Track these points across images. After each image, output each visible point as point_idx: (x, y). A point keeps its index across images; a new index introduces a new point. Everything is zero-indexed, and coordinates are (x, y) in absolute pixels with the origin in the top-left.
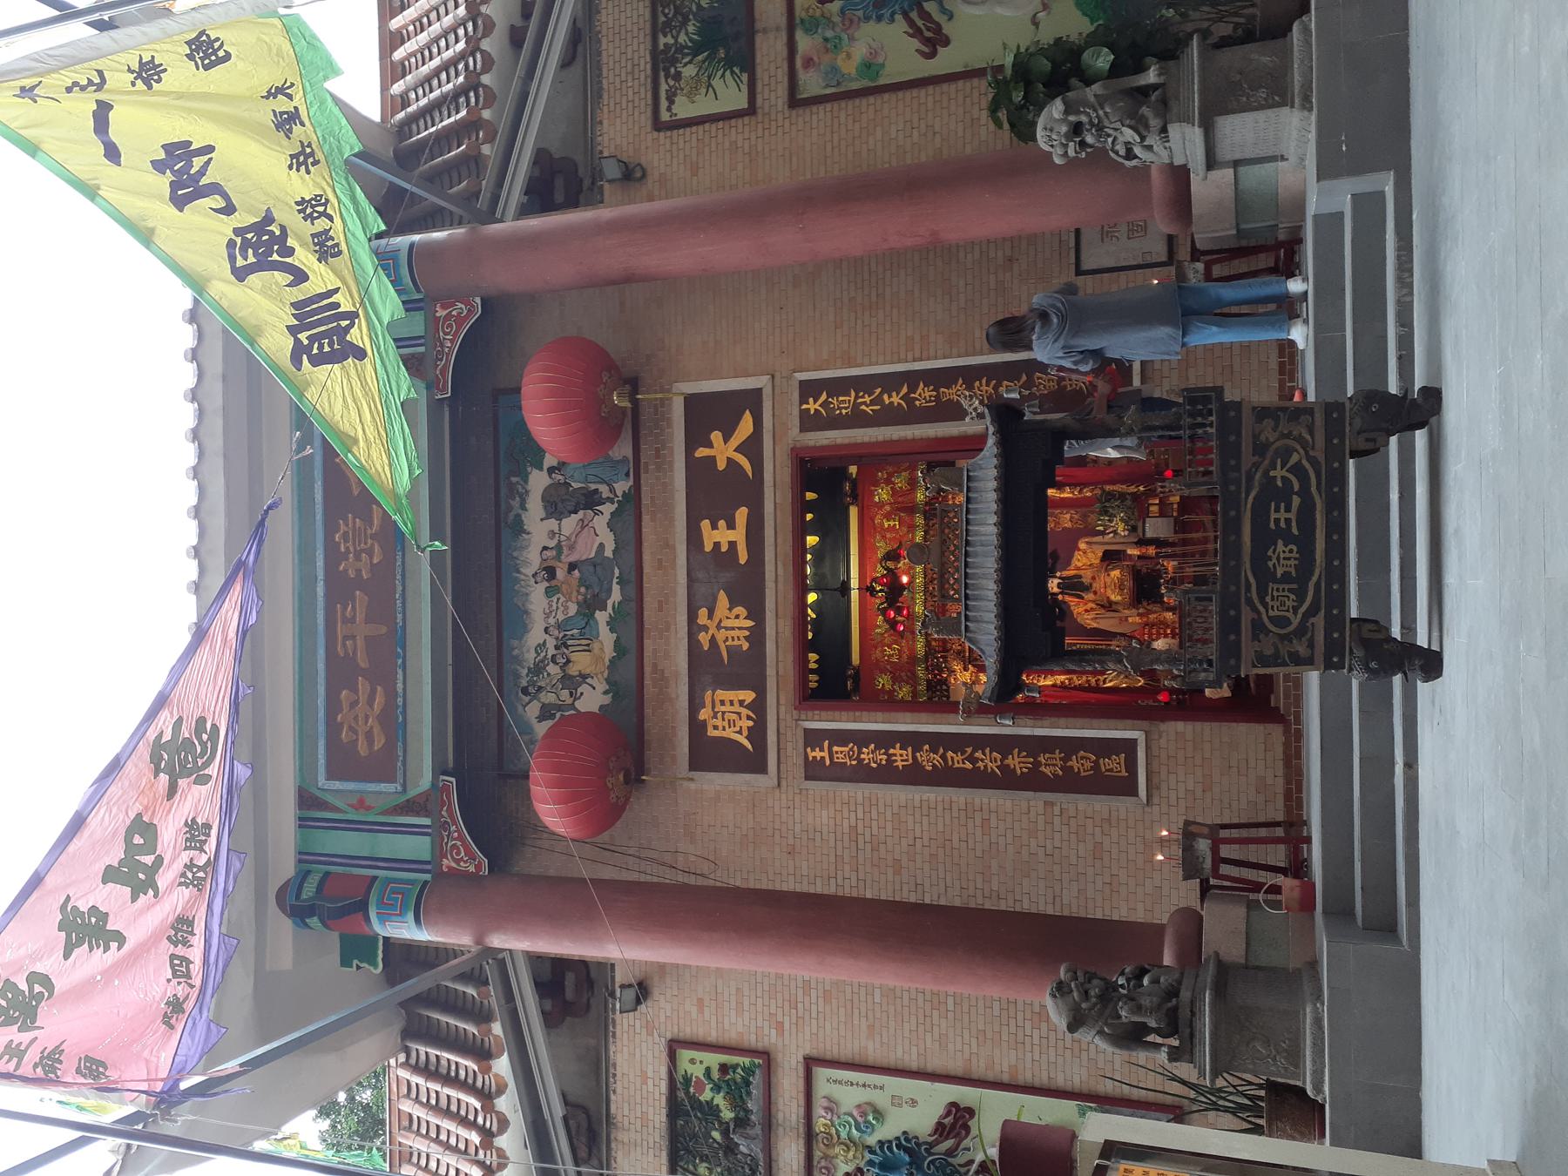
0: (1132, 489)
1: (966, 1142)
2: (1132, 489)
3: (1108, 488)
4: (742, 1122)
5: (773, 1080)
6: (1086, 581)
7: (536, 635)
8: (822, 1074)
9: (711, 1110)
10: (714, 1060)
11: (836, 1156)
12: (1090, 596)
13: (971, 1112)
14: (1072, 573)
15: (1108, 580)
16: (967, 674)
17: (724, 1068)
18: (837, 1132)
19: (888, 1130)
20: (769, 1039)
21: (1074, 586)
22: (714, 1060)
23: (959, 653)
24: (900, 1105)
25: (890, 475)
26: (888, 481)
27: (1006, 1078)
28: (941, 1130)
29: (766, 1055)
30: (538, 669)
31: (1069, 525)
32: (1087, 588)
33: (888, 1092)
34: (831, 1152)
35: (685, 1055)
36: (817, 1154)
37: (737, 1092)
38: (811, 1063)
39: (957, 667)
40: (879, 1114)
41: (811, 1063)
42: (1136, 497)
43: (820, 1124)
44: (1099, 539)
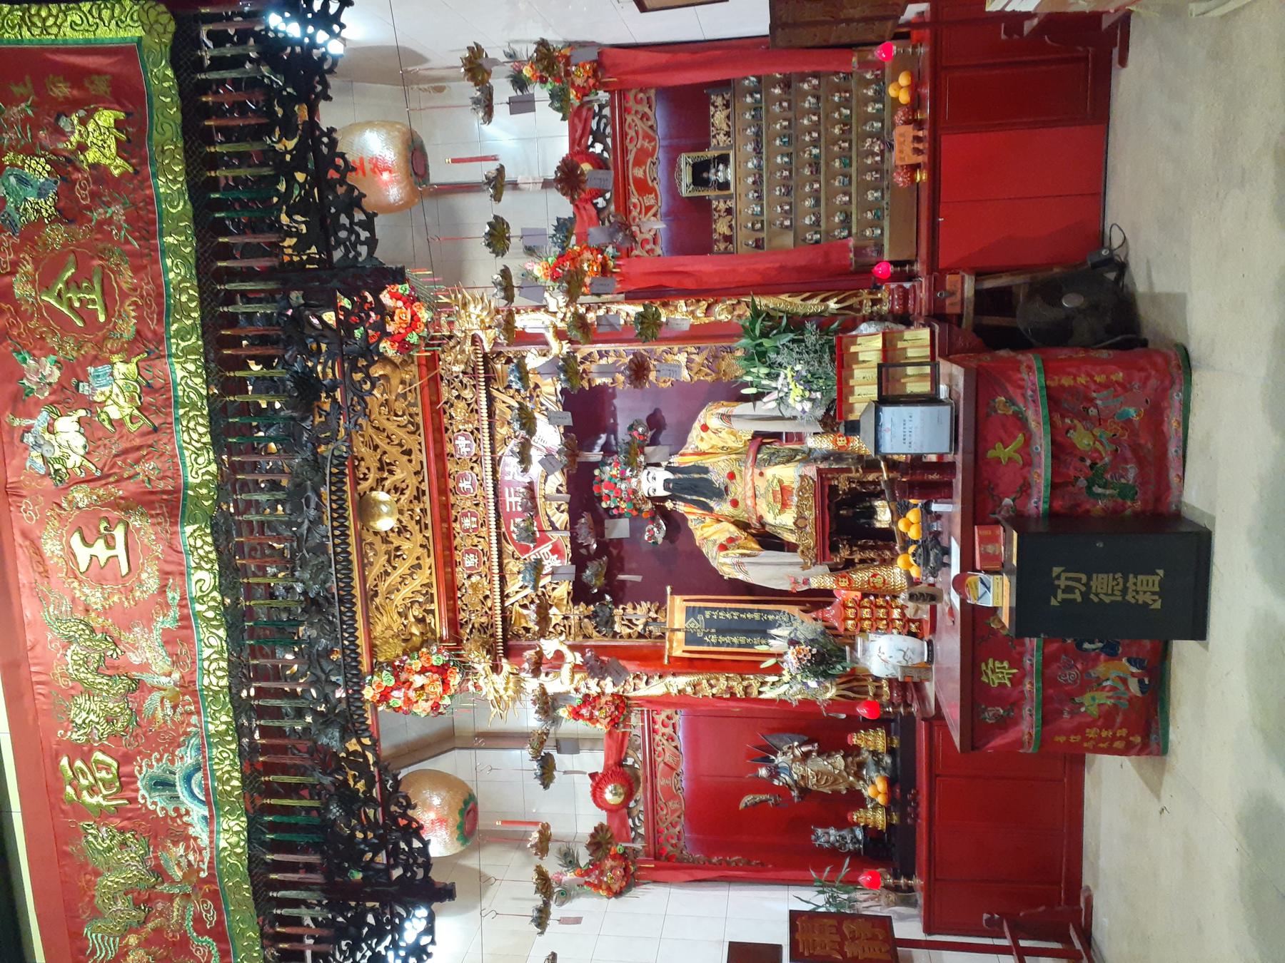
0: (814, 305)
2: (814, 305)
3: (763, 302)
6: (718, 476)
12: (724, 508)
14: (689, 461)
15: (761, 484)
16: (499, 680)
21: (695, 486)
23: (484, 628)
25: (73, 372)
26: (67, 396)
31: (685, 375)
32: (720, 494)
39: (481, 663)
42: (823, 322)
44: (744, 408)
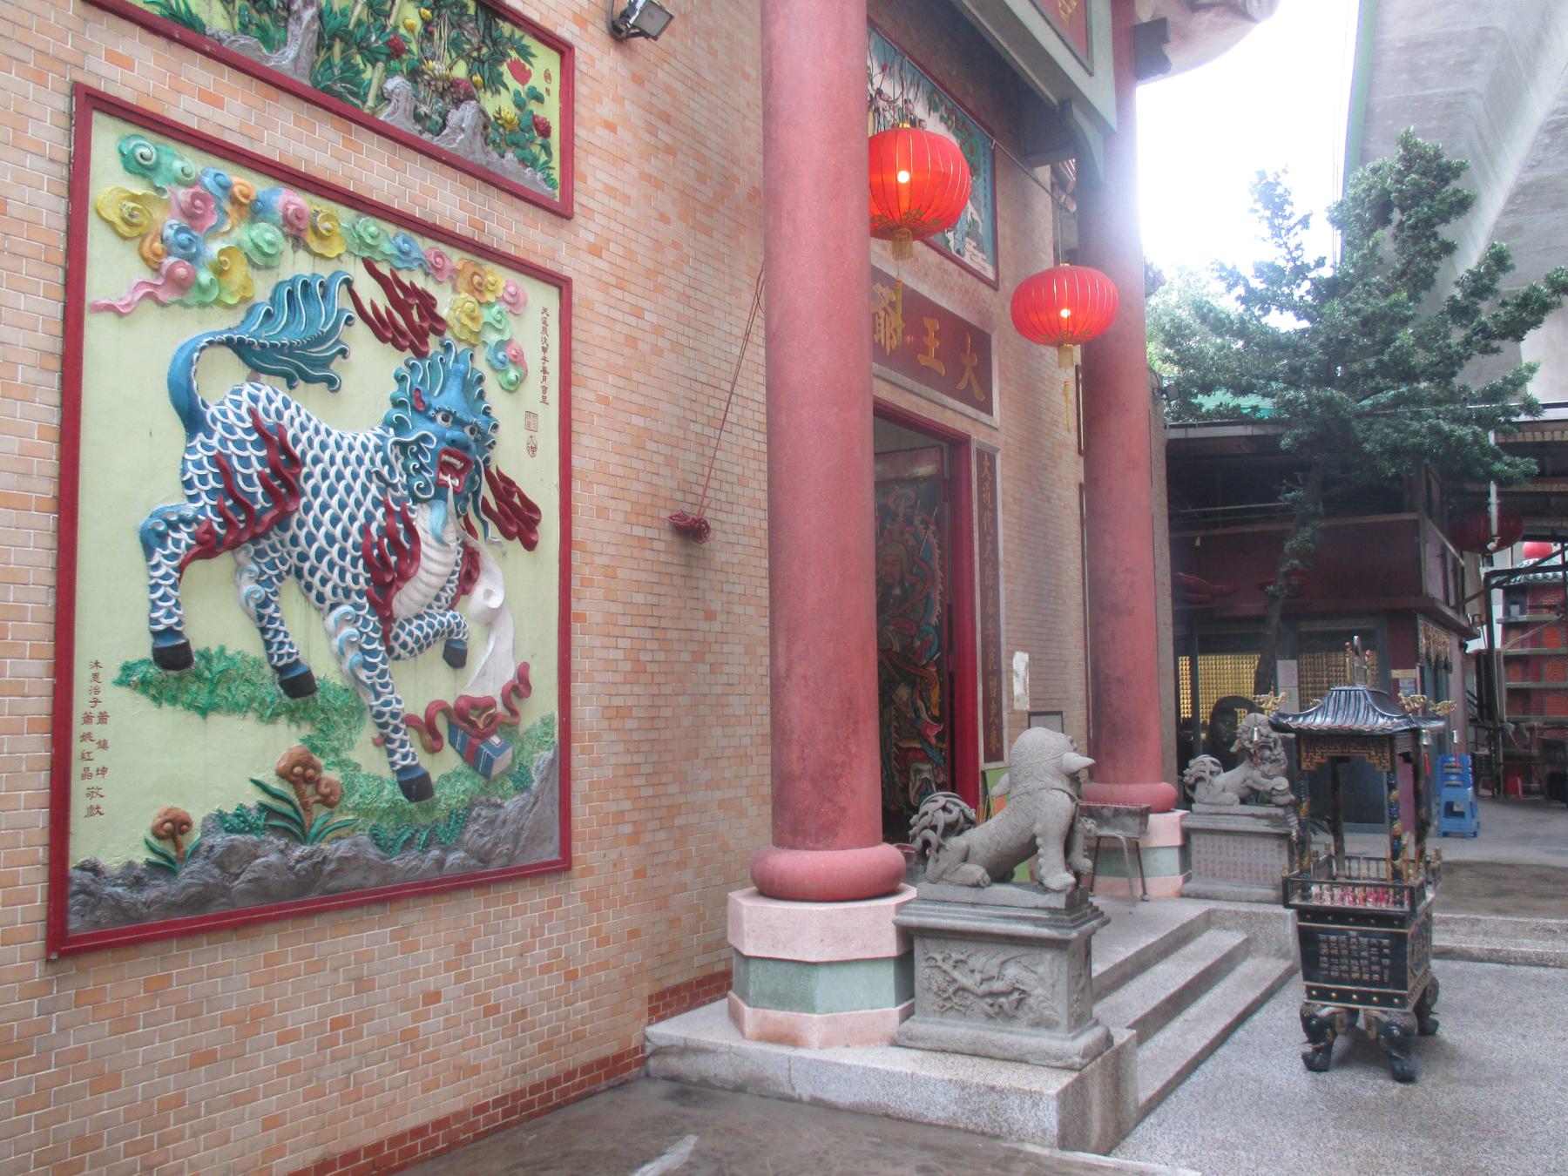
1: (493, 530)
5: (541, 213)
10: (550, 111)
11: (455, 290)
13: (530, 545)
17: (545, 131)
18: (489, 305)
20: (586, 230)
22: (550, 111)
24: (528, 427)
27: (576, 607)
28: (505, 487)
33: (539, 408)
34: (462, 282)
36: (456, 257)
40: (512, 388)
41: (561, 284)
43: (500, 277)
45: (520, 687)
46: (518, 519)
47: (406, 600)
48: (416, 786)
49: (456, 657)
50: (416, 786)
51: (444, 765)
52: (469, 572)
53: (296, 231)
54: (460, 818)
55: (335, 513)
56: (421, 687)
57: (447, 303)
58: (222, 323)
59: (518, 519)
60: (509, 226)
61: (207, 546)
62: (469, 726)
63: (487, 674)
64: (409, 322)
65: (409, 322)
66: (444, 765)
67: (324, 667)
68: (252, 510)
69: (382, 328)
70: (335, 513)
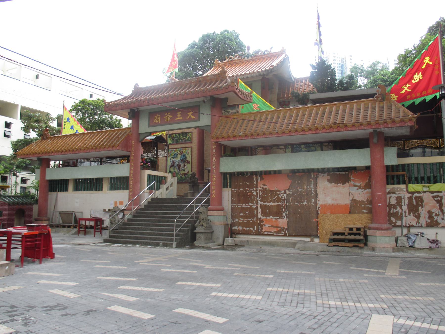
4: (186, 140)
7: (231, 111)
8: (190, 149)
9: (186, 137)
10: (191, 137)
19: (187, 156)
20: (193, 143)
28: (187, 161)
29: (192, 143)
30: (227, 112)
35: (191, 133)
37: (188, 140)
38: (192, 147)
41: (192, 147)
43: (187, 149)
45: (188, 172)
46: (188, 162)
47: (180, 168)
48: (182, 177)
49: (184, 171)
50: (182, 177)
51: (183, 176)
52: (185, 166)
53: (175, 151)
54: (184, 179)
55: (176, 164)
56: (182, 172)
57: (183, 151)
58: (172, 157)
59: (188, 162)
60: (187, 145)
61: (171, 167)
62: (185, 174)
63: (186, 171)
64: (182, 153)
65: (182, 153)
66: (183, 176)
67: (177, 172)
68: (173, 165)
69: (180, 154)
70: (176, 164)
